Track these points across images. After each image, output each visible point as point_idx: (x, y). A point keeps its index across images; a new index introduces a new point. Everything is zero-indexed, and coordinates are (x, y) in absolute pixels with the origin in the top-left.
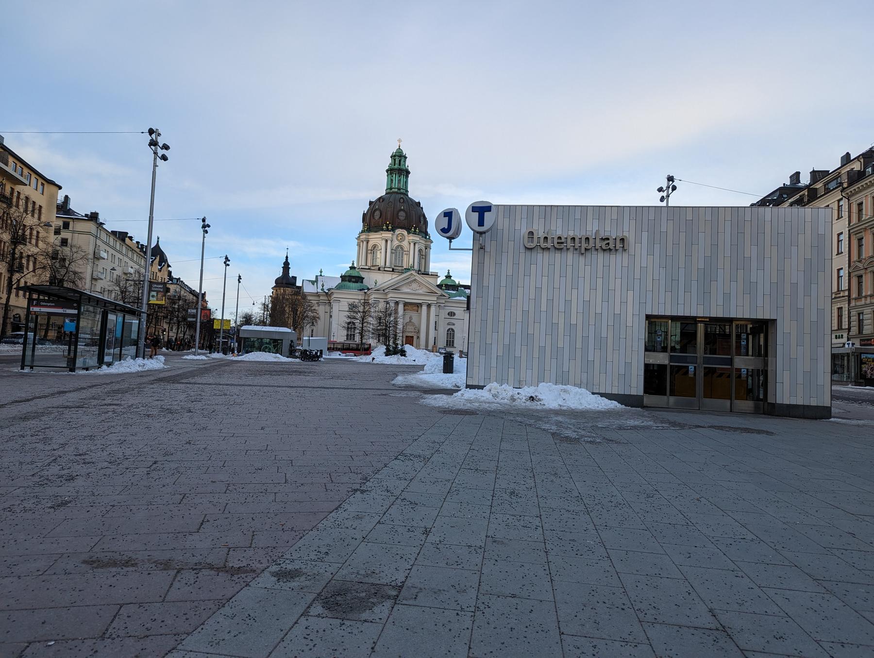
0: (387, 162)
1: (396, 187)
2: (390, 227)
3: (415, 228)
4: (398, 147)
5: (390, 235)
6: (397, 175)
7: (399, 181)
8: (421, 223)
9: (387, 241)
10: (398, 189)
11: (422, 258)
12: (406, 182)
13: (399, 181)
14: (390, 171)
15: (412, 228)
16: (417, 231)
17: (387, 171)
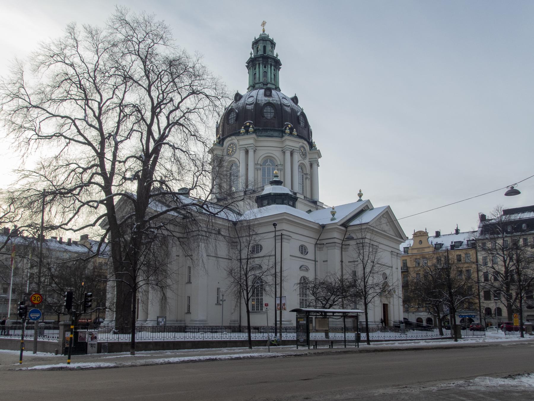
0: (248, 53)
1: (261, 80)
2: (251, 129)
3: (291, 129)
4: (262, 32)
5: (251, 141)
6: (261, 65)
7: (265, 73)
8: (299, 123)
9: (247, 152)
10: (264, 84)
11: (306, 178)
12: (276, 77)
13: (265, 73)
14: (252, 63)
15: (286, 129)
16: (295, 132)
17: (248, 63)
